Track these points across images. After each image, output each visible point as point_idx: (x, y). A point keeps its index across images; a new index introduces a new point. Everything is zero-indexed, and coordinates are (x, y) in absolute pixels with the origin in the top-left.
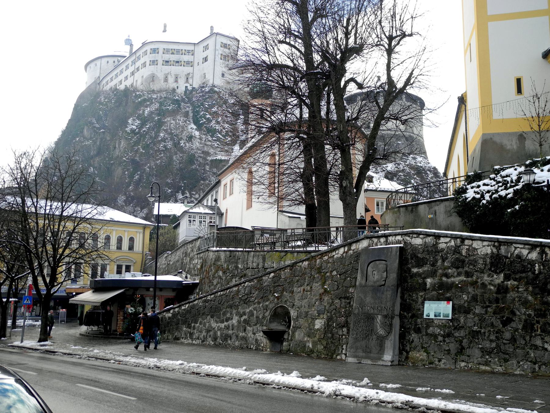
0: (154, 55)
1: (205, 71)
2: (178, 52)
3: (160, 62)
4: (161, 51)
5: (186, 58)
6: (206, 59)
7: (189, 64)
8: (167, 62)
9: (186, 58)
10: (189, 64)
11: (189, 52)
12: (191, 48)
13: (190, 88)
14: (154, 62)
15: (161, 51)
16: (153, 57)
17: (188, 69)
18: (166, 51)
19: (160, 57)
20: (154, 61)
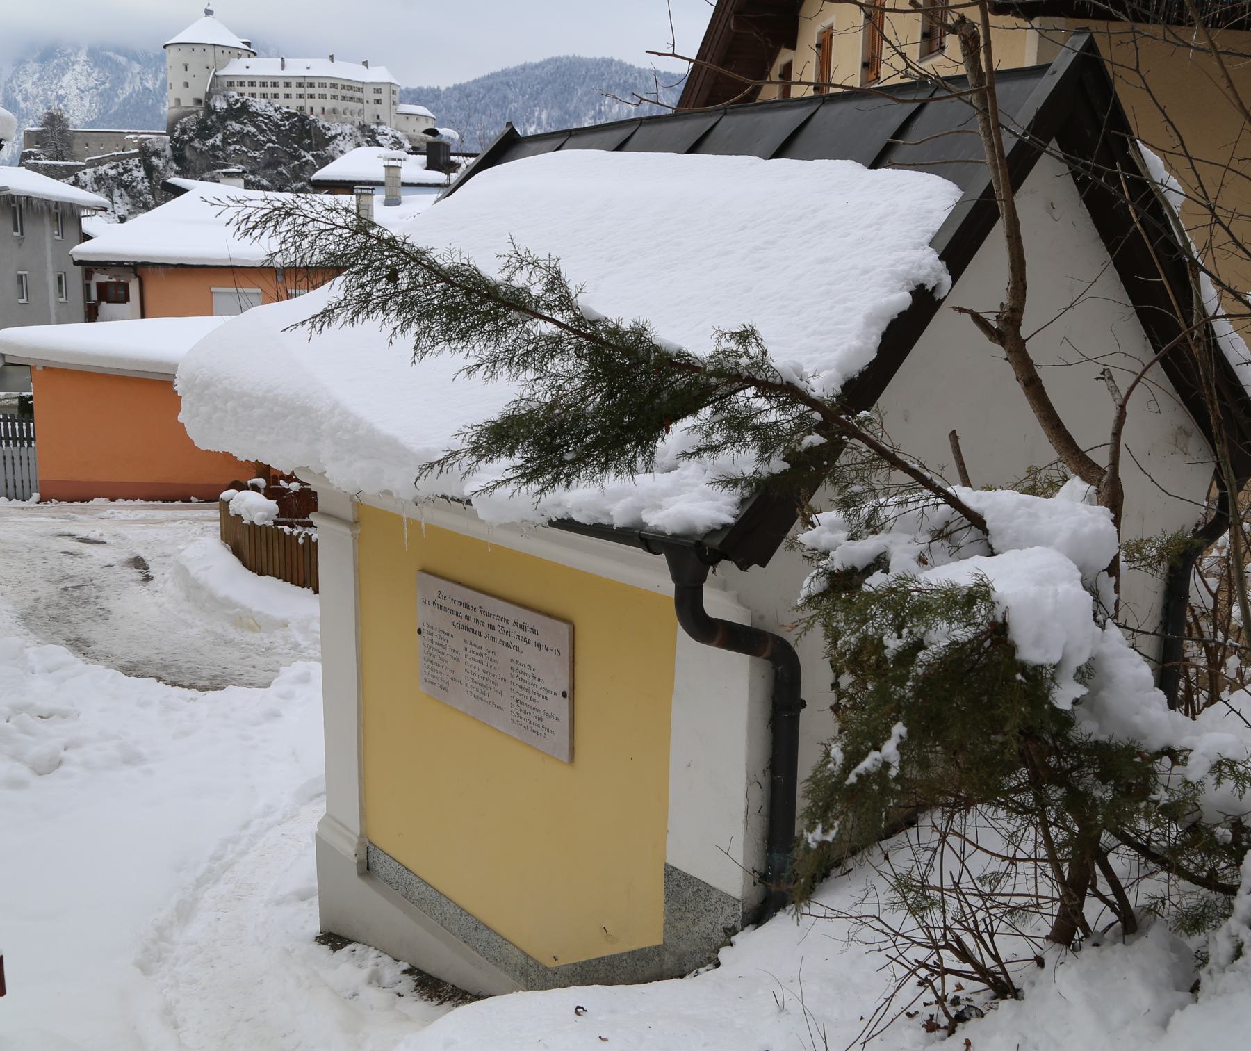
0: (333, 89)
1: (378, 113)
2: (351, 88)
3: (340, 97)
4: (339, 87)
5: (358, 95)
6: (378, 102)
7: (360, 100)
8: (344, 97)
9: (358, 95)
10: (360, 100)
11: (359, 89)
12: (360, 86)
13: (362, 123)
14: (334, 97)
15: (339, 87)
16: (333, 91)
17: (359, 106)
18: (343, 87)
19: (340, 92)
20: (334, 96)
